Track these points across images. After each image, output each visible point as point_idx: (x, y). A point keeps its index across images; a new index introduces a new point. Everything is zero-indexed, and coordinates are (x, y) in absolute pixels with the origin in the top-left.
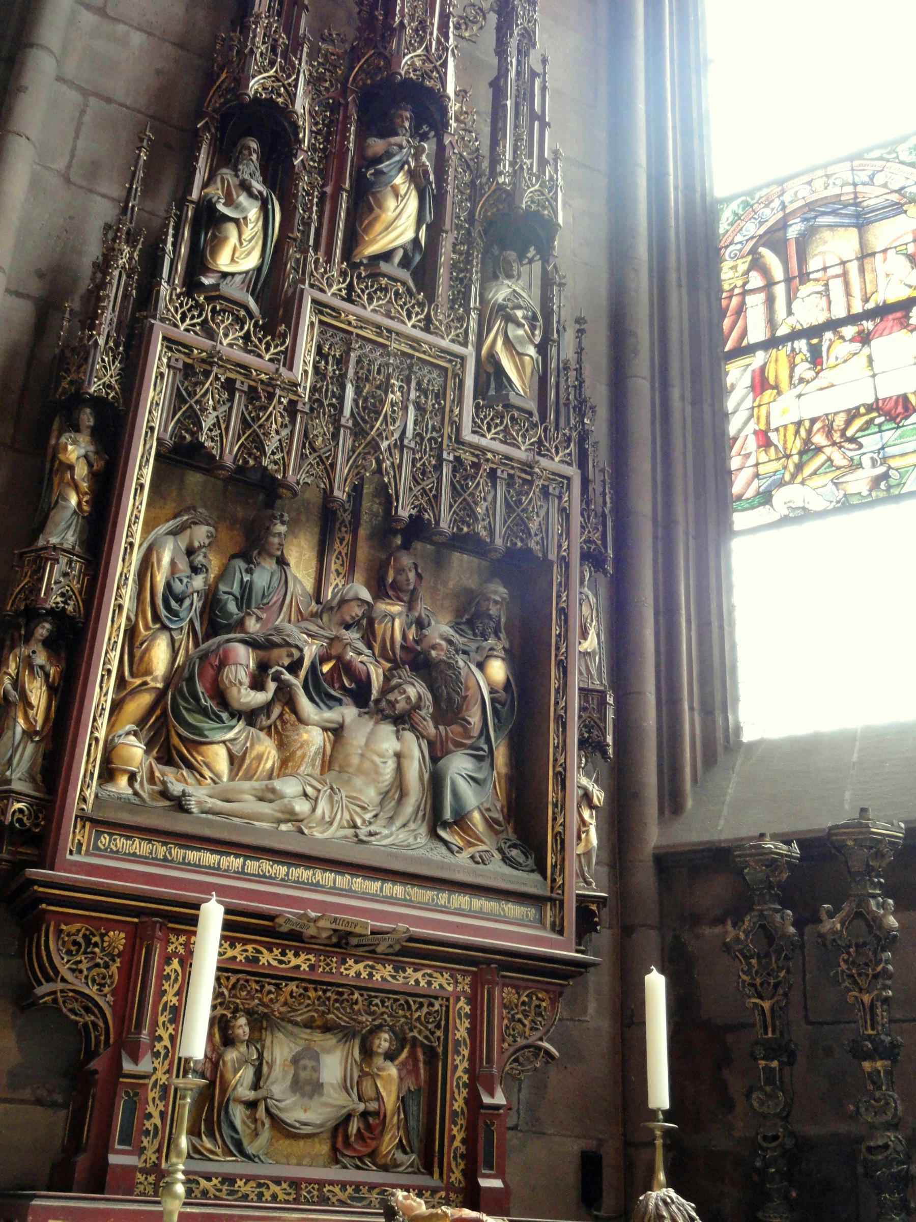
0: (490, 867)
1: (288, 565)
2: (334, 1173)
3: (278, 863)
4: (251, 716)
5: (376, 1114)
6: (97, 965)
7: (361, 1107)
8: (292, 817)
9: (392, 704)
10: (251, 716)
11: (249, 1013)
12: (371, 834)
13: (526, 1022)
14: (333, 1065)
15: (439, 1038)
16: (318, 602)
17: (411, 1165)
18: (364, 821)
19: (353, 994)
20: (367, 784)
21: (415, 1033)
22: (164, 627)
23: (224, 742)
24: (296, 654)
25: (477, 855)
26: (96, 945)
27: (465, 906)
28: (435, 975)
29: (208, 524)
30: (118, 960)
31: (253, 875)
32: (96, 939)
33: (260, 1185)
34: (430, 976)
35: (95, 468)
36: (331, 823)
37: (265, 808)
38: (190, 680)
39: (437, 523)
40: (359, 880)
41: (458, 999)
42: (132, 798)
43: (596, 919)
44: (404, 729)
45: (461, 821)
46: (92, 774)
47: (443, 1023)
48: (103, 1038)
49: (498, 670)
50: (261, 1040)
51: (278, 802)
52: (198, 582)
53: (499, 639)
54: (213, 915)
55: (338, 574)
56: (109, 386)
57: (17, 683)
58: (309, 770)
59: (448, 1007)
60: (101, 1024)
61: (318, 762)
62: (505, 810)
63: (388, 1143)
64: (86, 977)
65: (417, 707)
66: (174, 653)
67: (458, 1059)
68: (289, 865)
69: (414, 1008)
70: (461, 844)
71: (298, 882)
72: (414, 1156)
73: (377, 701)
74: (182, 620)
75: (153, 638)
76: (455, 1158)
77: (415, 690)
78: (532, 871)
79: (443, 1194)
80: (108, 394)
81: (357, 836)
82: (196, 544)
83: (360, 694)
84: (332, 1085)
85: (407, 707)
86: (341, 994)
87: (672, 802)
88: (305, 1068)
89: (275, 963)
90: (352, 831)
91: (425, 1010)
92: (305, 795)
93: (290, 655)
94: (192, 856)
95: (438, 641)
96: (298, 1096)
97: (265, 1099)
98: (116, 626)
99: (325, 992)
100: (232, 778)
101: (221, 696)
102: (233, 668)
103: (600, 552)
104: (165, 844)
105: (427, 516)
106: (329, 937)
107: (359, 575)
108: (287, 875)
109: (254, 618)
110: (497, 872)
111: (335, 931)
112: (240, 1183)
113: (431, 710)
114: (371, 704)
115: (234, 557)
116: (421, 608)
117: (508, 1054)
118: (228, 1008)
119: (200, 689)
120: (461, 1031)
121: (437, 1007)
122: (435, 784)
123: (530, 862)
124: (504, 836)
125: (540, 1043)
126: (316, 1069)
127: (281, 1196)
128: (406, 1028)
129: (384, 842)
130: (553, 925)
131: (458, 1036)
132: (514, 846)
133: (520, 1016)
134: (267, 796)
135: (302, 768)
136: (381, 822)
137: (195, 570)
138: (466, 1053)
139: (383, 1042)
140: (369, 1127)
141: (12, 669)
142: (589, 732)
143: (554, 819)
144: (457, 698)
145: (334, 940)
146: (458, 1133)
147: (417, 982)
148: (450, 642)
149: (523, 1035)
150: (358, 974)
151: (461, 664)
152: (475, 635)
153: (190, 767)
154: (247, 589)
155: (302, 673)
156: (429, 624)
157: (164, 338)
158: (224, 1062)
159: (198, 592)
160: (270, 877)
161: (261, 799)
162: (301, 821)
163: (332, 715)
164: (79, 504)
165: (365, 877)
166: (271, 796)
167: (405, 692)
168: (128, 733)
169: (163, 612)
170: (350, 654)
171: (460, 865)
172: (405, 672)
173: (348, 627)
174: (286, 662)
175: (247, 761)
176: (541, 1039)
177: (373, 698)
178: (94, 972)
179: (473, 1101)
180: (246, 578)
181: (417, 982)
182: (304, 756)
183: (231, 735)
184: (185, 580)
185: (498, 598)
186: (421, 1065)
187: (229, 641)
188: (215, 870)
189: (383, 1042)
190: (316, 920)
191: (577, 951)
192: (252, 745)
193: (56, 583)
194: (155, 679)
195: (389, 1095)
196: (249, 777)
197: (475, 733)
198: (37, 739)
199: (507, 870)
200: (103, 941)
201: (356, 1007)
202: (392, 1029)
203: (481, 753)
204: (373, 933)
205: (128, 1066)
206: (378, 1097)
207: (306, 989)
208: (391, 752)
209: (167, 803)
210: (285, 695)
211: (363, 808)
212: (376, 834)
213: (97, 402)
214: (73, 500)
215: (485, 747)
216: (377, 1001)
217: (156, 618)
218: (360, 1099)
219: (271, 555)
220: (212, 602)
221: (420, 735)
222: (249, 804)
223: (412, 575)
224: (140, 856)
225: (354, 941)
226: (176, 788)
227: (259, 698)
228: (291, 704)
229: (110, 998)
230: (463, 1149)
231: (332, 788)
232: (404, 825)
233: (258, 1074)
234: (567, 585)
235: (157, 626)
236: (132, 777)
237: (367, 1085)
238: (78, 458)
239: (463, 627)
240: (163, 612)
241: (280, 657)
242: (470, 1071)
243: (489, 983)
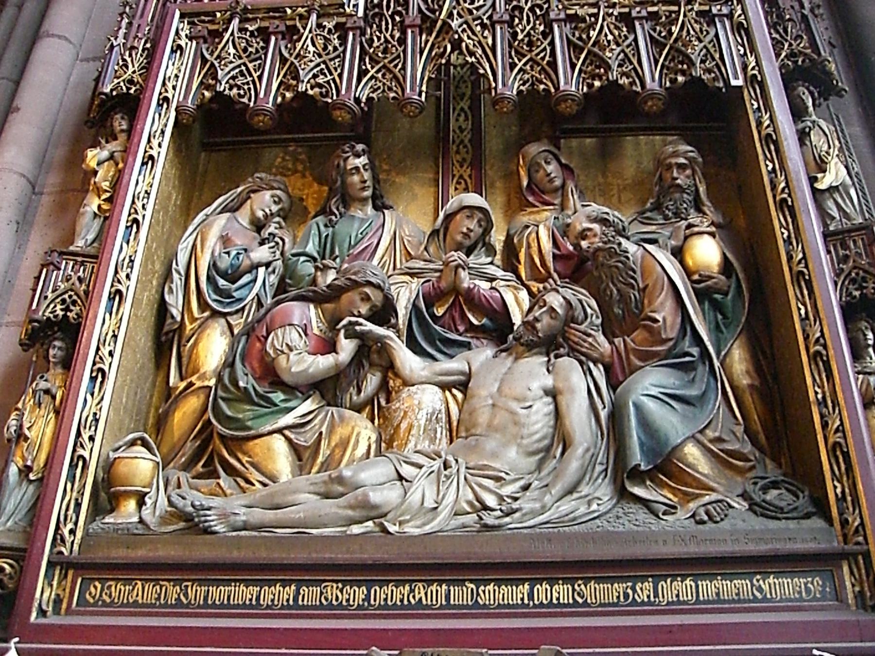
3: (352, 583)
8: (373, 512)
18: (501, 498)
20: (505, 445)
22: (215, 314)
23: (280, 431)
24: (376, 296)
25: (702, 511)
29: (272, 188)
31: (314, 607)
37: (330, 507)
39: (557, 88)
40: (491, 587)
45: (665, 466)
49: (707, 252)
53: (705, 213)
56: (131, 82)
71: (386, 607)
78: (807, 516)
80: (128, 89)
83: (498, 329)
92: (401, 478)
93: (366, 298)
94: (218, 593)
101: (270, 374)
103: (812, 60)
104: (177, 582)
105: (542, 87)
108: (367, 598)
123: (803, 502)
132: (775, 485)
143: (825, 425)
144: (634, 294)
148: (604, 222)
153: (231, 471)
161: (326, 496)
165: (499, 582)
169: (210, 297)
174: (364, 309)
182: (410, 427)
185: (682, 160)
194: (203, 377)
197: (672, 333)
199: (758, 523)
209: (182, 524)
210: (371, 353)
219: (364, 200)
221: (584, 358)
224: (143, 605)
227: (325, 362)
232: (570, 492)
235: (206, 314)
239: (648, 214)
240: (210, 297)
241: (352, 303)
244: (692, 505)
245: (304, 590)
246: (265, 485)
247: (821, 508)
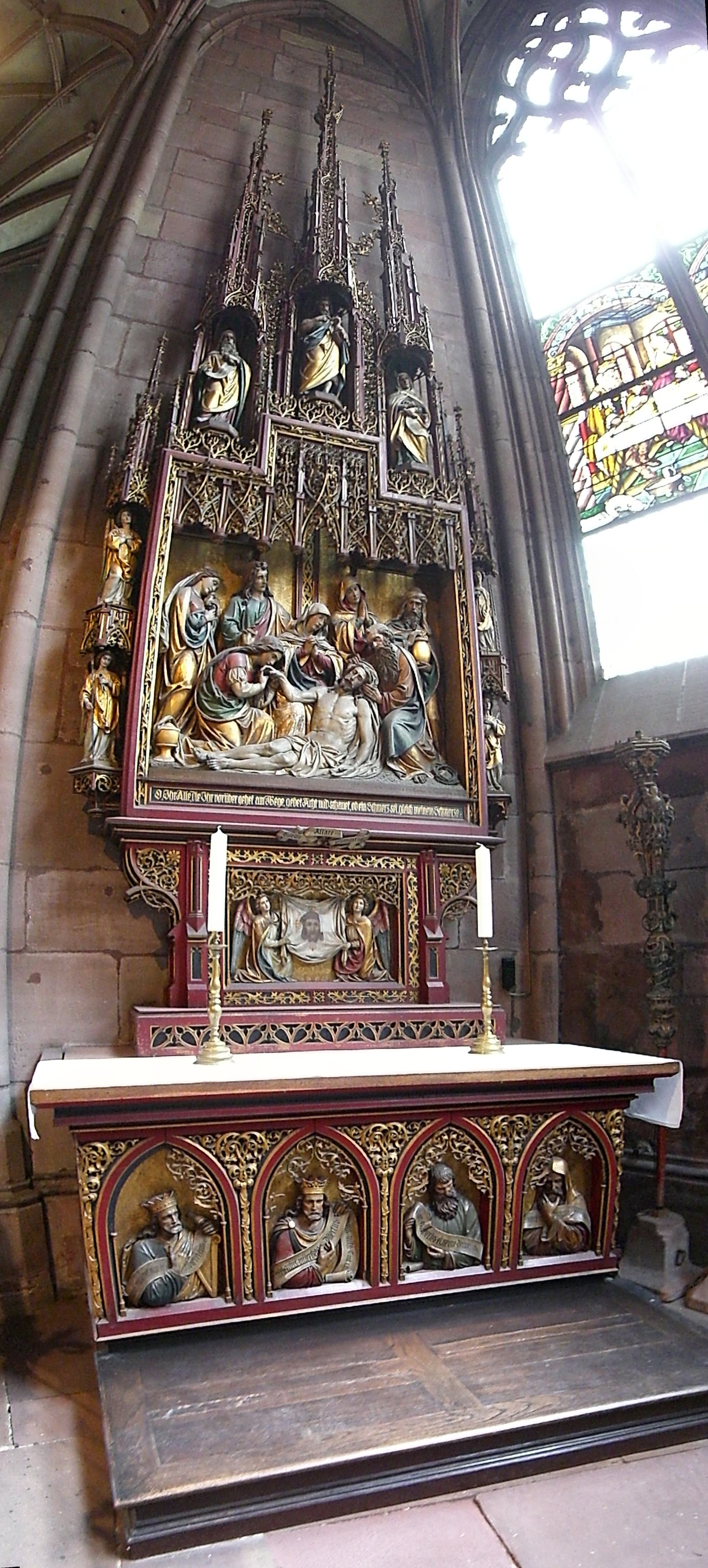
0: (425, 784)
1: (272, 596)
2: (336, 984)
4: (252, 700)
5: (359, 949)
6: (165, 873)
7: (349, 945)
8: (284, 765)
9: (349, 682)
10: (252, 700)
11: (269, 894)
12: (340, 771)
13: (456, 885)
14: (328, 922)
15: (397, 899)
16: (295, 618)
17: (384, 977)
18: (336, 763)
19: (336, 876)
20: (336, 738)
21: (381, 897)
22: (189, 648)
23: (235, 720)
26: (161, 860)
27: (410, 812)
28: (391, 859)
29: (214, 576)
30: (177, 869)
32: (162, 857)
33: (287, 995)
34: (388, 860)
35: (132, 549)
36: (312, 766)
37: (266, 761)
38: (208, 681)
39: (369, 554)
40: (335, 802)
41: (408, 874)
42: (174, 764)
43: (503, 812)
44: (359, 698)
45: (403, 756)
46: (145, 752)
47: (399, 889)
48: (175, 917)
49: (424, 650)
50: (280, 909)
51: (275, 756)
52: (210, 615)
54: (219, 841)
55: (308, 598)
57: (92, 698)
58: (297, 732)
59: (402, 879)
60: (173, 908)
61: (303, 726)
62: (437, 744)
63: (368, 964)
64: (158, 881)
65: (367, 682)
66: (198, 664)
67: (410, 911)
68: (285, 797)
69: (378, 882)
70: (405, 771)
71: (292, 807)
72: (385, 972)
73: (339, 681)
74: (201, 642)
75: (182, 655)
76: (412, 970)
77: (364, 669)
78: (456, 784)
79: (405, 992)
81: (330, 772)
82: (207, 590)
83: (329, 678)
84: (328, 933)
85: (360, 682)
86: (329, 877)
87: (555, 728)
88: (310, 924)
89: (281, 861)
90: (328, 770)
91: (386, 882)
92: (293, 749)
93: (275, 657)
94: (219, 798)
95: (377, 635)
96: (307, 941)
97: (285, 945)
98: (151, 652)
99: (317, 877)
100: (243, 744)
101: (229, 690)
102: (235, 670)
104: (199, 792)
105: (361, 551)
106: (316, 842)
107: (323, 597)
109: (250, 636)
110: (432, 787)
111: (319, 837)
112: (273, 994)
113: (377, 683)
114: (336, 683)
115: (234, 595)
116: (365, 613)
117: (444, 906)
118: (253, 892)
119: (214, 686)
120: (412, 894)
121: (394, 880)
122: (383, 733)
123: (455, 777)
124: (435, 762)
125: (466, 897)
126: (317, 924)
127: (301, 1000)
128: (374, 895)
129: (350, 775)
130: (472, 818)
131: (410, 897)
132: (444, 768)
133: (452, 881)
134: (266, 753)
135: (291, 732)
136: (347, 761)
137: (208, 608)
138: (416, 907)
139: (360, 904)
140: (355, 957)
141: (88, 688)
142: (491, 685)
143: (469, 748)
144: (394, 673)
145: (319, 843)
146: (413, 956)
147: (379, 865)
148: (385, 635)
149: (455, 893)
150: (339, 863)
151: (395, 648)
152: (406, 628)
153: (213, 738)
154: (243, 615)
155: (286, 668)
156: (373, 623)
157: (174, 459)
158: (256, 925)
159: (211, 622)
160: (273, 806)
161: (262, 755)
162: (291, 767)
163: (309, 694)
164: (123, 574)
165: (338, 800)
166: (269, 753)
167: (357, 672)
168: (167, 722)
169: (186, 638)
170: (318, 651)
171: (405, 784)
172: (357, 659)
173: (315, 634)
174: (273, 662)
175: (253, 731)
176: (467, 894)
177: (337, 679)
178: (163, 876)
179: (422, 936)
180: (243, 608)
181: (379, 865)
182: (291, 723)
183: (239, 714)
184: (199, 615)
185: (419, 601)
186: (387, 917)
187: (231, 652)
188: (235, 805)
189: (360, 904)
190: (304, 832)
191: (490, 835)
192: (255, 720)
193: (110, 628)
194: (185, 683)
195: (366, 936)
196: (253, 741)
198: (108, 732)
200: (166, 858)
201: (339, 885)
202: (365, 896)
203: (415, 708)
204: (344, 836)
205: (191, 932)
206: (359, 939)
207: (304, 876)
208: (351, 715)
209: (198, 765)
210: (275, 685)
211: (334, 754)
212: (344, 770)
213: (132, 507)
214: (119, 572)
215: (418, 704)
216: (354, 879)
217: (182, 642)
218: (348, 940)
220: (221, 627)
221: (370, 700)
222: (255, 759)
223: (357, 592)
225: (333, 843)
226: (203, 755)
227: (256, 688)
228: (280, 689)
229: (175, 892)
230: (417, 965)
231: (311, 743)
232: (364, 763)
233: (280, 929)
234: (465, 588)
235: (184, 648)
236: (173, 751)
237: (351, 932)
238: (120, 545)
240: (186, 638)
241: (268, 659)
242: (419, 918)
243: (428, 862)
244: (412, 774)
245: (257, 798)
246: (231, 748)
247: (462, 781)
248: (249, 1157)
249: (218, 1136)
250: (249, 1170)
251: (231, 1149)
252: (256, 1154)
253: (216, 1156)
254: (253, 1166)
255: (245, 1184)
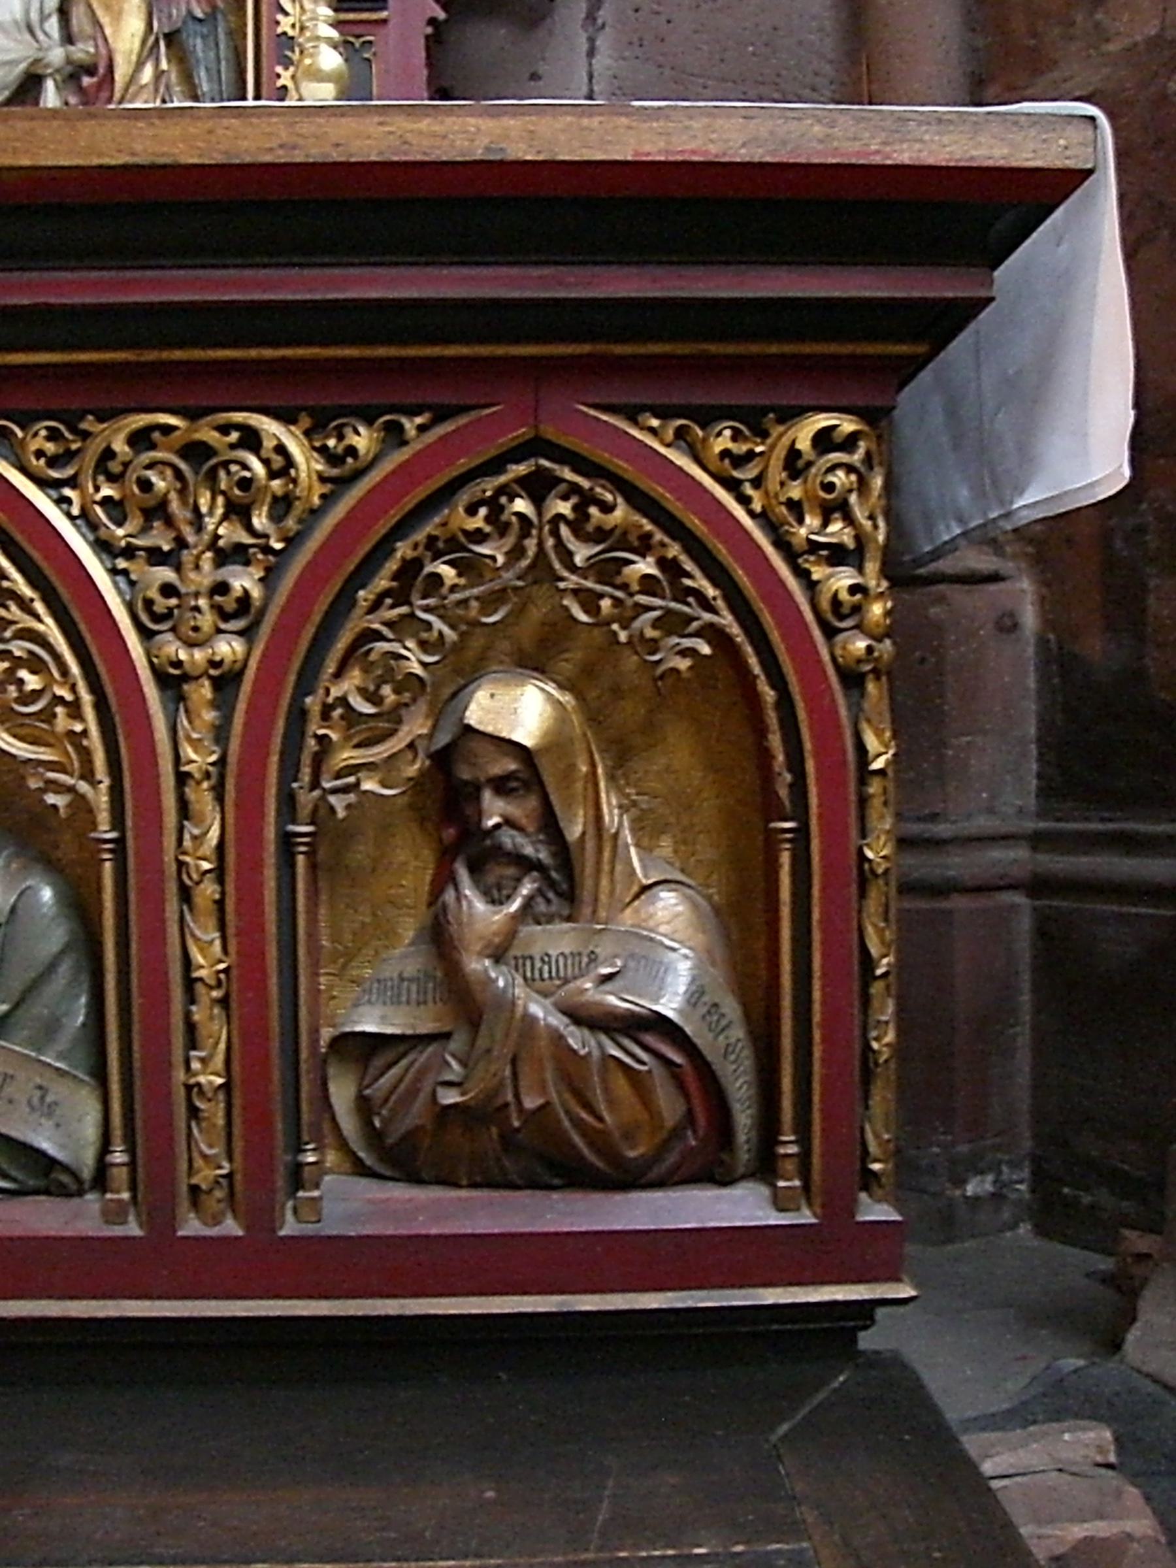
248: (231, 533)
249: (88, 424)
250: (222, 588)
251: (146, 485)
252: (260, 521)
253: (84, 519)
254: (244, 580)
255: (199, 655)
